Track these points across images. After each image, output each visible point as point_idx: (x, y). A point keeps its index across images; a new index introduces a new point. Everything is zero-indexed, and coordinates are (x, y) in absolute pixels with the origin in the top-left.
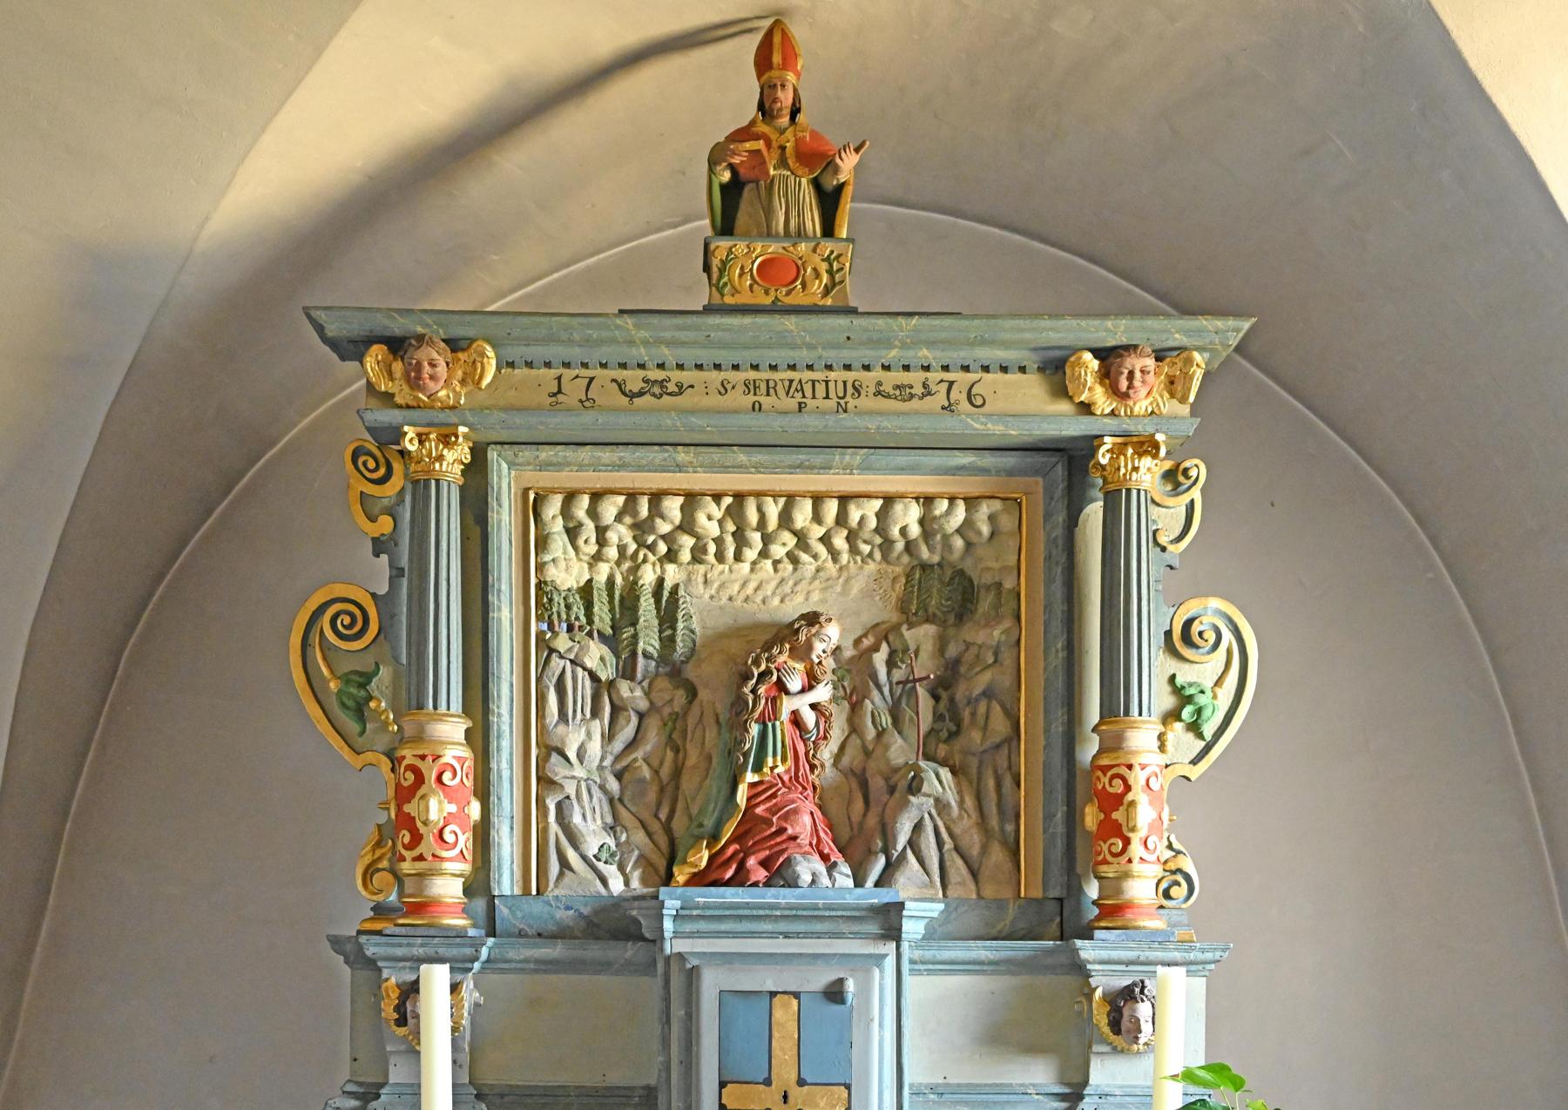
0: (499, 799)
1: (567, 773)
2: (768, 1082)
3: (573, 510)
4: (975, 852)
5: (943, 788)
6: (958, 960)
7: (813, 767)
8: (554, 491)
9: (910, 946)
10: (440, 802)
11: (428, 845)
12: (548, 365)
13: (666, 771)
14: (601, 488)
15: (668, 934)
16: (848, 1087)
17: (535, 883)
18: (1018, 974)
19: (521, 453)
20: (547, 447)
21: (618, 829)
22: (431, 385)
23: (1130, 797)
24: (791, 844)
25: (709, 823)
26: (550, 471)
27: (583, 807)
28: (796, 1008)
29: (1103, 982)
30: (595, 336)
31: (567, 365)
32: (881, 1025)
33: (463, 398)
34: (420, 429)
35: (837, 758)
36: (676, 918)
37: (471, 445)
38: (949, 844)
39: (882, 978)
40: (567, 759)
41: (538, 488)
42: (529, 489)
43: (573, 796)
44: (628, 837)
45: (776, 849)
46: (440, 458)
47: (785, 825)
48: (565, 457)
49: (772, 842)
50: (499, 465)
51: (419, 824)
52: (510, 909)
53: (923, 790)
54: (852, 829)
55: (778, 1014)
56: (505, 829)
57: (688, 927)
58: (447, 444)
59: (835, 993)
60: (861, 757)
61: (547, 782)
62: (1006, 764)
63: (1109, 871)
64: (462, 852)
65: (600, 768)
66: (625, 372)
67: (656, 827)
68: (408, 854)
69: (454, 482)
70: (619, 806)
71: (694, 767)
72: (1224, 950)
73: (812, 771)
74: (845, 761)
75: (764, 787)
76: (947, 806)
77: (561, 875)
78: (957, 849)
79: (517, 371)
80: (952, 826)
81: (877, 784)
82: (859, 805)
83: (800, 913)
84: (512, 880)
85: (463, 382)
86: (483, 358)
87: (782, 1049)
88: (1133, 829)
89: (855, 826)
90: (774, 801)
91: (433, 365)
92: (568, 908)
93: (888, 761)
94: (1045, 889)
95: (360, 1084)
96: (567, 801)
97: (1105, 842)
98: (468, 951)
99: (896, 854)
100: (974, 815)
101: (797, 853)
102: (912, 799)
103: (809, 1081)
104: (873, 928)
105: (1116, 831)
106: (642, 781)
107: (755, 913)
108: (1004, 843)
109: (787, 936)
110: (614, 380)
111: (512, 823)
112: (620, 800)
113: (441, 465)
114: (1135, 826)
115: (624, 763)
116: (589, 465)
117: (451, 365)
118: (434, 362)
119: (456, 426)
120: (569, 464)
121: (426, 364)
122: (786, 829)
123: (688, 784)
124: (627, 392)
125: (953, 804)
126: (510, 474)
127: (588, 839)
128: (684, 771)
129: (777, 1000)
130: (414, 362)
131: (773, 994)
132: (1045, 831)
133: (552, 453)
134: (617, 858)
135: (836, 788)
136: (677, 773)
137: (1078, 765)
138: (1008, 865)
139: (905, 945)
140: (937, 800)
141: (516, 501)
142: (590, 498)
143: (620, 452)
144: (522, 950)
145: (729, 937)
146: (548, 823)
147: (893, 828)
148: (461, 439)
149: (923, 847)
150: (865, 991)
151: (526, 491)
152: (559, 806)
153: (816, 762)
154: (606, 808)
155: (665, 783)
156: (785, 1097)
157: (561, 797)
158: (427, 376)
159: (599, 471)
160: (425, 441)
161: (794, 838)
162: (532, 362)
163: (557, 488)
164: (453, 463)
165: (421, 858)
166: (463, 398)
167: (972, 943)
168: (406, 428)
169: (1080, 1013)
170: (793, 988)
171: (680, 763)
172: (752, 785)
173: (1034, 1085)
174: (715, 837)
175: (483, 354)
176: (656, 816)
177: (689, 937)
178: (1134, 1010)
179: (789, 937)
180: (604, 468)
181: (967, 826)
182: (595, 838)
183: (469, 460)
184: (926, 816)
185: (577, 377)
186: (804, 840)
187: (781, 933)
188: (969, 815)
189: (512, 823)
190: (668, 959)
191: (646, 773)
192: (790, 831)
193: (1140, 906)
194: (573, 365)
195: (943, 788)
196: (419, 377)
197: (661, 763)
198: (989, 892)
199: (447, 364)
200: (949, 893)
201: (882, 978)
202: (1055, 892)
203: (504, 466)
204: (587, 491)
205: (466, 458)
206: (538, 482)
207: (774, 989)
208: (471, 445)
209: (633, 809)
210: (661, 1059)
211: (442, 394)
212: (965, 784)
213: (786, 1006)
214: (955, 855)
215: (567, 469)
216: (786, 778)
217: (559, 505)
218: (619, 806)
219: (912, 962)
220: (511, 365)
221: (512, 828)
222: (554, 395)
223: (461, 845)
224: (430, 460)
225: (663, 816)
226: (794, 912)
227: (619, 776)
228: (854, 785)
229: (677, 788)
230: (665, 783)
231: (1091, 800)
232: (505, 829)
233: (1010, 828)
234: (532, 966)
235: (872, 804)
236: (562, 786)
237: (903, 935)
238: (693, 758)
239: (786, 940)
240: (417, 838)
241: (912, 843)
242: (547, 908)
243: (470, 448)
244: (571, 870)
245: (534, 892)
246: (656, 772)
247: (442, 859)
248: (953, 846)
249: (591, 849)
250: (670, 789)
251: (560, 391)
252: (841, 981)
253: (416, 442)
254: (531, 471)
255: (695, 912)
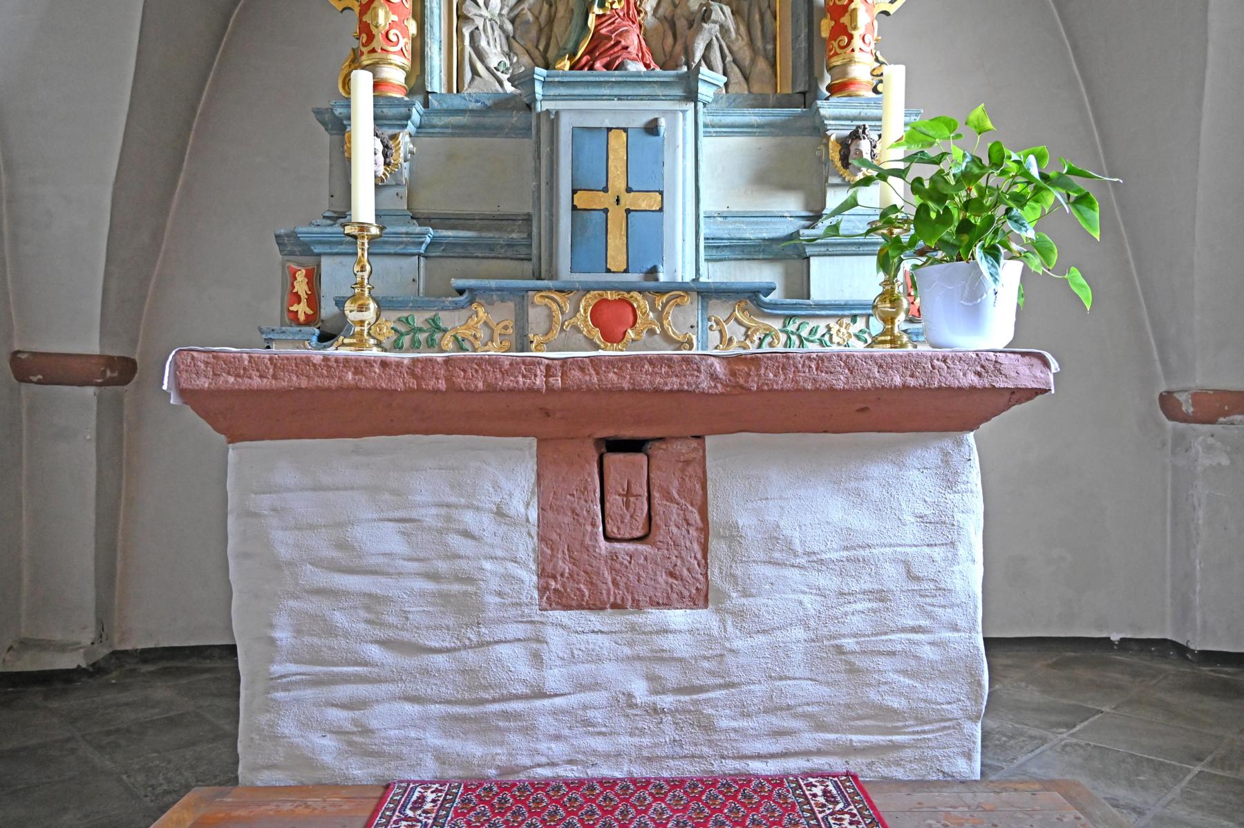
0: (431, 27)
1: (478, 12)
2: (606, 190)
4: (747, 62)
5: (725, 17)
6: (737, 124)
7: (639, 12)
9: (704, 113)
10: (386, 13)
11: (379, 42)
13: (543, 18)
15: (538, 96)
16: (661, 193)
17: (456, 82)
18: (777, 135)
21: (512, 54)
23: (852, 6)
24: (625, 55)
25: (570, 45)
27: (487, 37)
28: (625, 139)
29: (835, 133)
32: (684, 157)
35: (656, 10)
36: (544, 83)
38: (729, 58)
39: (684, 125)
40: (477, 4)
43: (481, 28)
44: (518, 60)
45: (614, 56)
47: (620, 39)
49: (612, 52)
51: (372, 28)
52: (438, 102)
53: (712, 18)
54: (665, 56)
55: (613, 143)
56: (435, 48)
57: (553, 92)
59: (652, 129)
60: (671, 8)
61: (463, 18)
62: (767, 4)
63: (837, 61)
64: (402, 49)
65: (500, 15)
67: (536, 54)
68: (365, 50)
70: (512, 40)
71: (563, 17)
72: (917, 115)
73: (639, 14)
74: (661, 11)
75: (607, 18)
76: (728, 31)
77: (473, 79)
78: (735, 61)
80: (731, 45)
81: (681, 24)
82: (670, 40)
83: (629, 79)
84: (440, 84)
87: (616, 167)
88: (855, 28)
89: (667, 53)
90: (613, 26)
92: (477, 101)
93: (688, 8)
94: (793, 88)
95: (335, 212)
96: (477, 31)
97: (835, 41)
98: (403, 110)
99: (694, 65)
100: (746, 39)
101: (628, 59)
102: (705, 25)
103: (634, 189)
104: (678, 92)
105: (843, 31)
106: (528, 22)
107: (597, 79)
108: (766, 58)
109: (620, 98)
111: (440, 45)
112: (514, 37)
114: (856, 25)
115: (516, 12)
122: (620, 42)
123: (558, 29)
125: (732, 30)
127: (491, 56)
128: (556, 20)
129: (611, 134)
131: (609, 129)
132: (793, 49)
134: (511, 71)
135: (656, 29)
136: (551, 20)
137: (815, 4)
138: (769, 71)
139: (700, 105)
140: (722, 26)
144: (443, 118)
145: (580, 100)
146: (464, 45)
147: (693, 46)
149: (712, 58)
150: (672, 127)
152: (472, 35)
153: (641, 9)
154: (504, 41)
155: (543, 26)
156: (618, 201)
157: (472, 28)
161: (626, 48)
165: (373, 51)
167: (746, 111)
169: (821, 157)
170: (623, 125)
171: (553, 14)
172: (598, 17)
173: (788, 212)
174: (575, 54)
176: (537, 47)
177: (553, 100)
178: (859, 146)
179: (621, 99)
181: (741, 46)
182: (495, 57)
184: (714, 38)
186: (633, 49)
187: (616, 96)
188: (743, 39)
189: (440, 45)
190: (539, 115)
191: (530, 17)
192: (623, 43)
193: (859, 83)
195: (725, 17)
197: (540, 13)
198: (756, 88)
200: (729, 90)
201: (684, 125)
202: (801, 89)
207: (610, 126)
209: (522, 43)
210: (534, 183)
212: (739, 19)
213: (618, 137)
214: (733, 65)
216: (621, 14)
218: (512, 40)
219: (706, 126)
221: (440, 49)
223: (402, 43)
225: (541, 48)
226: (624, 79)
227: (513, 21)
228: (667, 25)
229: (551, 31)
230: (543, 26)
231: (825, 17)
232: (435, 48)
233: (770, 47)
234: (450, 131)
235: (678, 36)
236: (473, 20)
237: (699, 96)
238: (561, 11)
239: (620, 102)
240: (371, 37)
241: (705, 58)
242: (463, 102)
244: (480, 76)
245: (455, 91)
246: (537, 18)
247: (388, 51)
248: (731, 59)
249: (493, 64)
250: (546, 29)
252: (656, 120)
255: (557, 79)
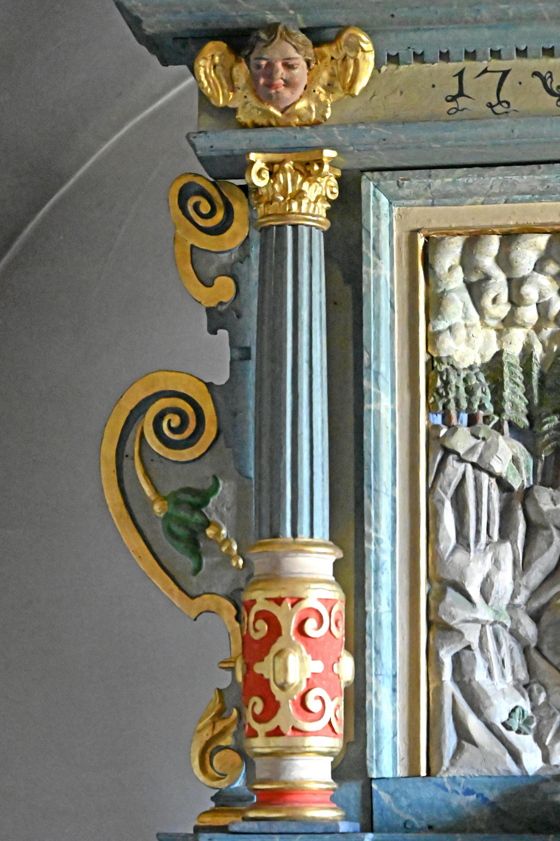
3: (477, 257)
8: (451, 233)
12: (445, 56)
14: (517, 225)
19: (406, 182)
20: (442, 172)
22: (286, 93)
26: (446, 205)
30: (511, 13)
31: (471, 56)
33: (329, 109)
34: (271, 157)
37: (339, 174)
41: (430, 230)
42: (418, 231)
46: (299, 195)
48: (466, 184)
50: (377, 200)
58: (308, 175)
66: (552, 61)
69: (317, 228)
79: (402, 68)
85: (329, 88)
86: (357, 52)
91: (288, 66)
110: (536, 74)
113: (300, 205)
116: (500, 194)
117: (313, 65)
118: (290, 63)
119: (321, 149)
120: (471, 194)
121: (279, 65)
124: (555, 89)
126: (391, 211)
130: (264, 63)
133: (450, 180)
141: (399, 248)
142: (501, 241)
143: (543, 173)
148: (326, 168)
151: (414, 233)
158: (282, 82)
159: (514, 202)
160: (278, 172)
162: (422, 53)
163: (456, 228)
164: (316, 202)
166: (329, 109)
168: (253, 156)
175: (357, 47)
180: (519, 197)
183: (337, 195)
185: (485, 71)
194: (479, 55)
196: (270, 85)
199: (308, 63)
203: (384, 200)
204: (497, 230)
205: (332, 193)
206: (430, 221)
208: (339, 174)
211: (301, 105)
215: (470, 201)
217: (458, 251)
220: (394, 59)
222: (454, 98)
224: (285, 198)
243: (337, 179)
251: (461, 93)
253: (266, 174)
254: (420, 206)
